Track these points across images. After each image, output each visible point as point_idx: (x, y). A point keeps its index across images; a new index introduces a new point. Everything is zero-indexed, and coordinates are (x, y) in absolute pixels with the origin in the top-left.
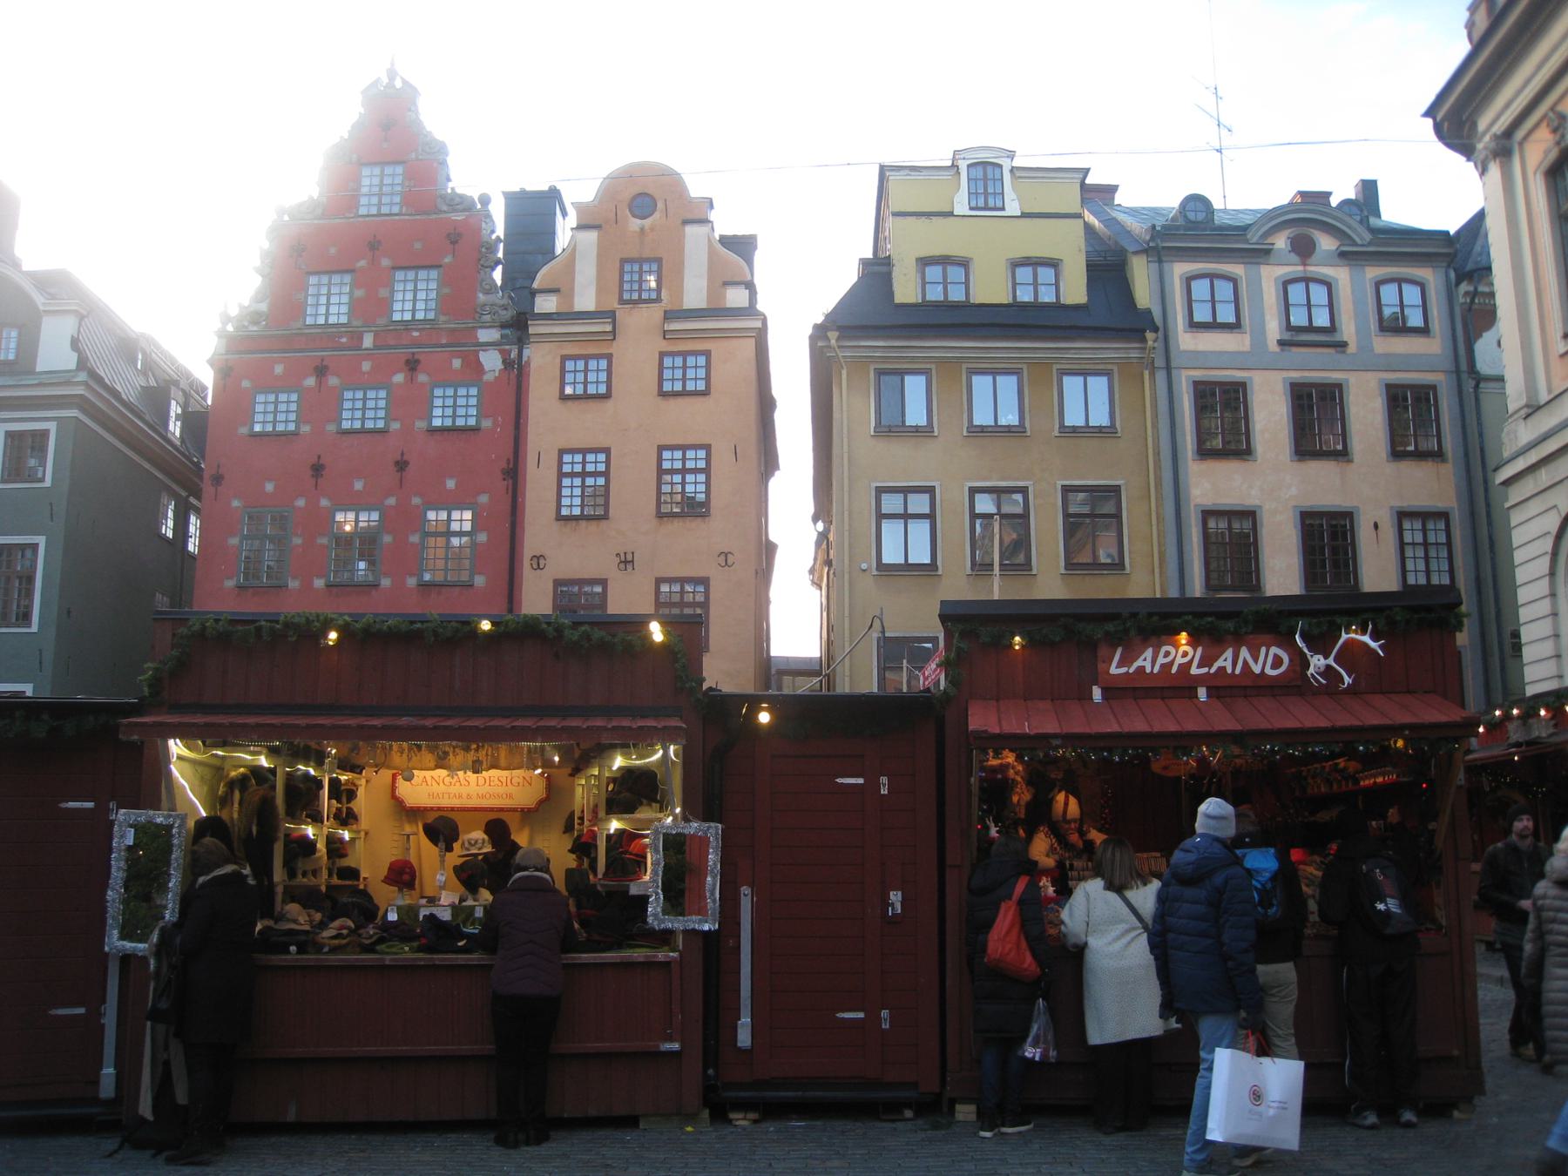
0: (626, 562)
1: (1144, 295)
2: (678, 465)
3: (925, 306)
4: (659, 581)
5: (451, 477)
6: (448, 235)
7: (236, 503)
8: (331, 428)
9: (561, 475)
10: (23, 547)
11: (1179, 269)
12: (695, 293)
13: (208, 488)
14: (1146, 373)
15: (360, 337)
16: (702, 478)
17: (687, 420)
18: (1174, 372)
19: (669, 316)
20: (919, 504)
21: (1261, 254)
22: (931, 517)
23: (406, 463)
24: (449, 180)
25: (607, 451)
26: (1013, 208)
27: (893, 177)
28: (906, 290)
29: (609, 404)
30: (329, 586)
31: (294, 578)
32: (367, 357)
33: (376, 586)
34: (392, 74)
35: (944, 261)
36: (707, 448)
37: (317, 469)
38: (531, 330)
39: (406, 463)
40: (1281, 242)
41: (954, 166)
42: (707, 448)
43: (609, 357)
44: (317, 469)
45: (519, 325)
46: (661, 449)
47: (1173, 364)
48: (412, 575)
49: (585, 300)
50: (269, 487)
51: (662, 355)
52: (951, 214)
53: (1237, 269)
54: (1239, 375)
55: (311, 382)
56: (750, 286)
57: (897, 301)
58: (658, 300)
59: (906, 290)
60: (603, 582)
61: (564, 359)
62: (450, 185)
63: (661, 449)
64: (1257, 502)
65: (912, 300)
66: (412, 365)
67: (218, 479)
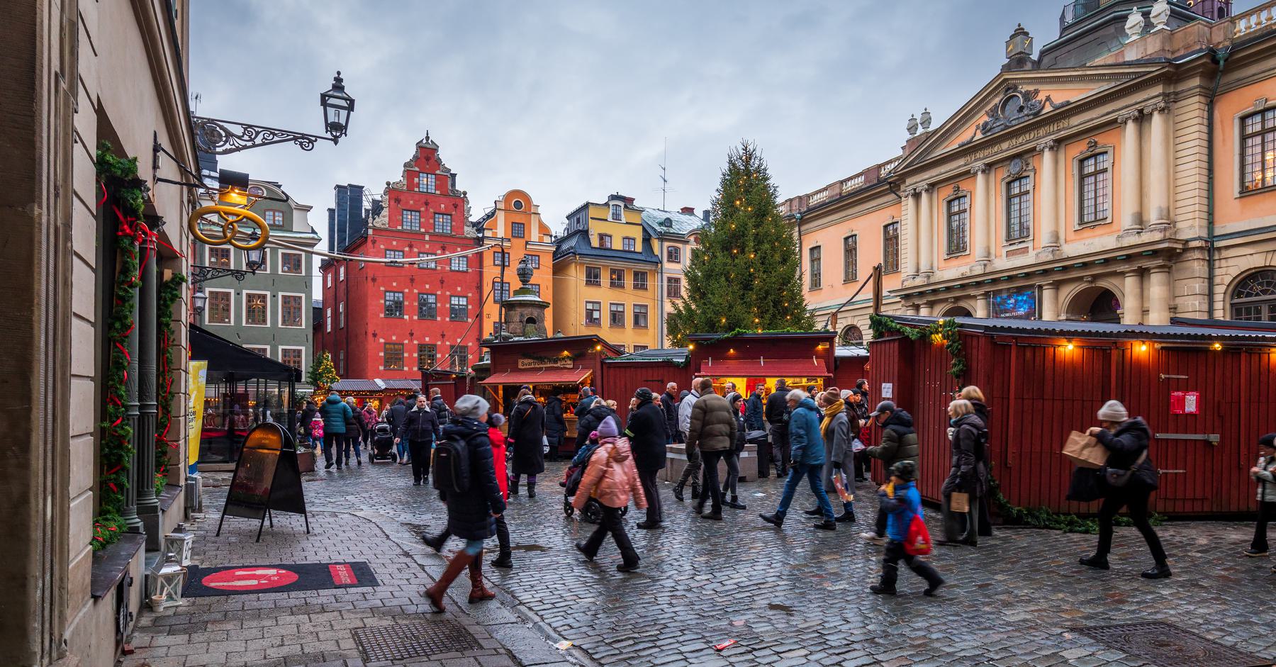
1: (657, 251)
10: (294, 297)
11: (666, 244)
19: (527, 243)
20: (596, 307)
21: (687, 242)
26: (624, 220)
27: (591, 207)
28: (595, 242)
34: (427, 138)
37: (412, 280)
40: (692, 239)
44: (412, 280)
53: (680, 245)
55: (407, 249)
67: (374, 280)
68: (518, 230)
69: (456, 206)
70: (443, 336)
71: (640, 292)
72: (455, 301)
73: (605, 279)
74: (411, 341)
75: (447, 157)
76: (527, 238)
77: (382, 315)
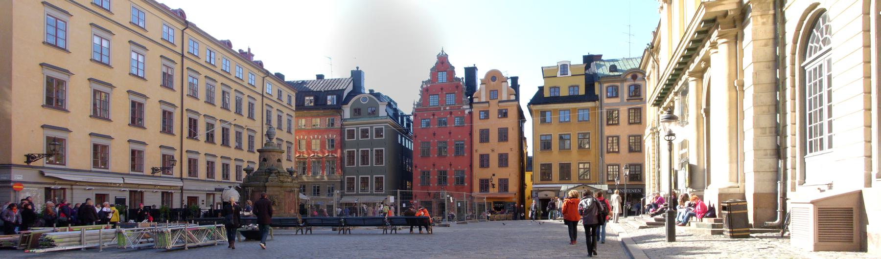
49: (483, 100)
59: (547, 94)
66: (451, 113)
68: (494, 94)
69: (457, 87)
75: (452, 61)
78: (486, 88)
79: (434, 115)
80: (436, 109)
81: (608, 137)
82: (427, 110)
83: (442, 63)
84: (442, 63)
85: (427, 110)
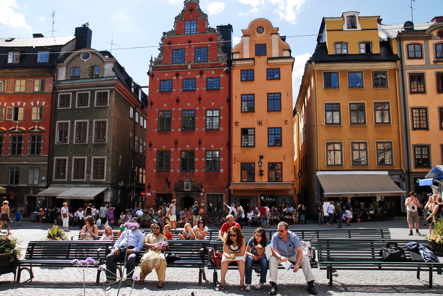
0: (260, 123)
1: (395, 51)
2: (273, 98)
3: (336, 55)
4: (269, 128)
5: (213, 102)
6: (209, 39)
7: (157, 110)
8: (181, 90)
9: (242, 101)
12: (275, 53)
13: (149, 105)
14: (396, 72)
15: (187, 66)
16: (279, 101)
17: (274, 87)
18: (404, 71)
22: (339, 111)
23: (201, 98)
24: (208, 24)
25: (254, 95)
26: (359, 27)
28: (331, 51)
29: (254, 82)
30: (182, 130)
31: (173, 128)
32: (189, 71)
33: (195, 130)
35: (341, 43)
36: (280, 93)
37: (178, 100)
38: (233, 63)
39: (201, 98)
41: (342, 16)
42: (280, 93)
43: (253, 70)
44: (178, 100)
45: (230, 62)
46: (268, 94)
47: (404, 69)
48: (203, 127)
49: (246, 55)
50: (165, 105)
51: (267, 69)
52: (342, 30)
54: (422, 71)
55: (175, 78)
56: (290, 51)
57: (329, 53)
58: (266, 55)
60: (254, 129)
61: (241, 71)
62: (209, 26)
63: (268, 94)
64: (427, 106)
65: (333, 54)
66: (201, 73)
67: (152, 104)
68: (261, 50)
70: (200, 143)
71: (381, 91)
72: (209, 113)
73: (343, 82)
74: (176, 148)
76: (269, 55)
77: (156, 130)
78: (250, 42)
79: (177, 75)
80: (181, 68)
81: (413, 109)
82: (168, 68)
83: (191, 10)
84: (191, 10)
85: (168, 68)
